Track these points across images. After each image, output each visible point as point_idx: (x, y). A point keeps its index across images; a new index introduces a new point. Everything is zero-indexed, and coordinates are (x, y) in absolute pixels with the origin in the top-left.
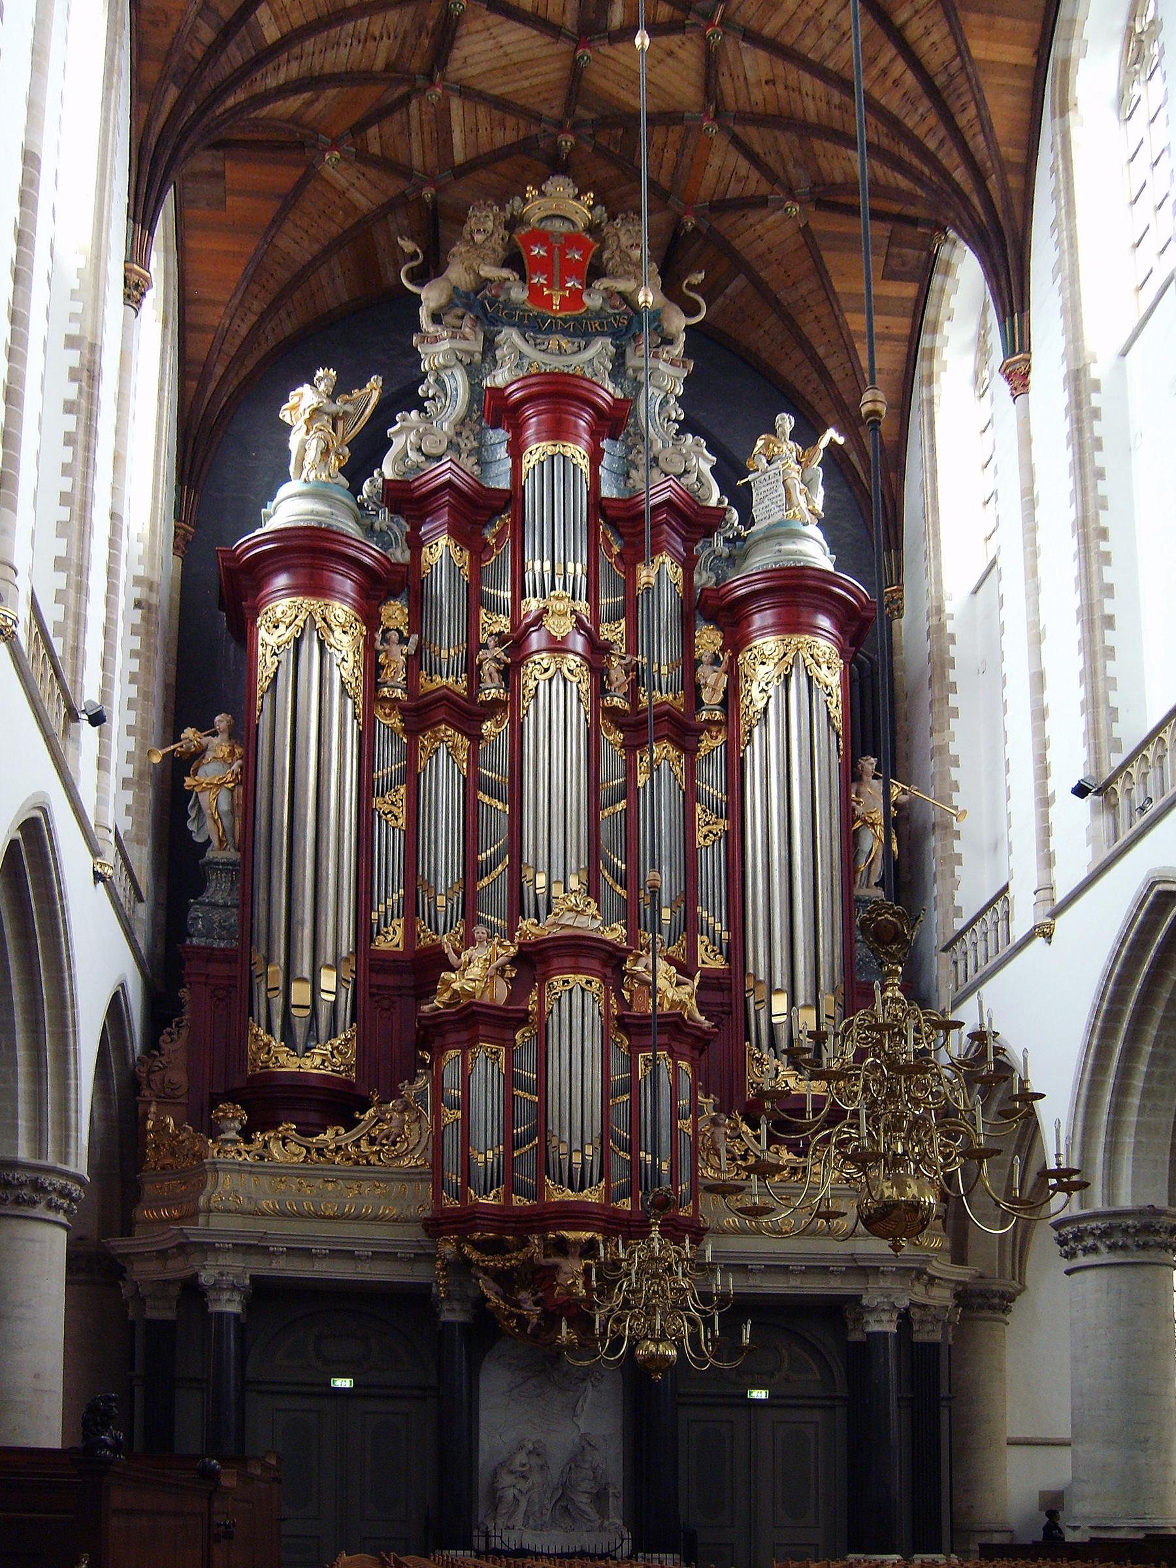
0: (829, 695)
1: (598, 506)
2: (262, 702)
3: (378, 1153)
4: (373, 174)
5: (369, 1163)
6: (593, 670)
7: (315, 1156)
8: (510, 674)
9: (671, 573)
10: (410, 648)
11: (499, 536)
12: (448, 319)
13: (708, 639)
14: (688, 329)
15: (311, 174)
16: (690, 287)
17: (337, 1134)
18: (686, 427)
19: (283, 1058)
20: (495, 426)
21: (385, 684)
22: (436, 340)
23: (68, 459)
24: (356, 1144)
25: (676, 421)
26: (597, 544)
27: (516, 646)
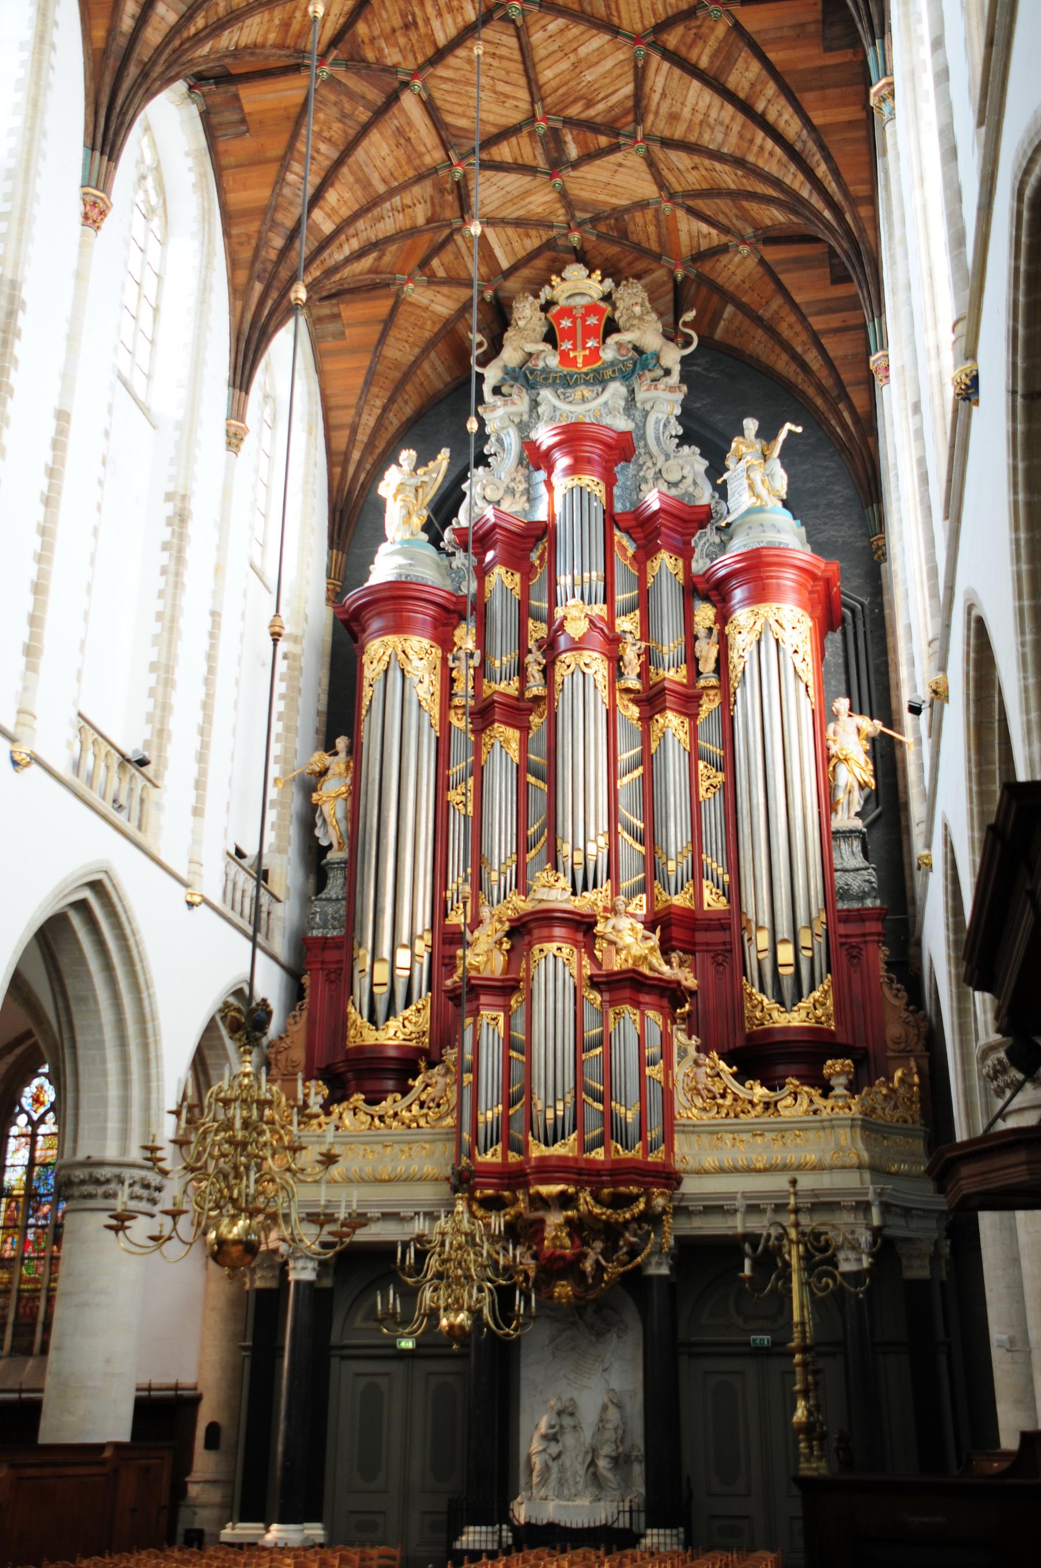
0: (796, 652)
1: (611, 519)
2: (364, 727)
3: (426, 1115)
4: (445, 290)
5: (418, 1127)
6: (610, 659)
7: (377, 1121)
8: (547, 672)
9: (670, 567)
10: (476, 662)
11: (541, 558)
12: (505, 390)
13: (705, 614)
14: (684, 361)
15: (398, 302)
16: (685, 324)
17: (395, 1101)
18: (684, 440)
19: (365, 1032)
20: (538, 469)
21: (456, 694)
22: (494, 408)
23: (162, 586)
24: (409, 1108)
25: (676, 436)
26: (612, 551)
27: (550, 648)
